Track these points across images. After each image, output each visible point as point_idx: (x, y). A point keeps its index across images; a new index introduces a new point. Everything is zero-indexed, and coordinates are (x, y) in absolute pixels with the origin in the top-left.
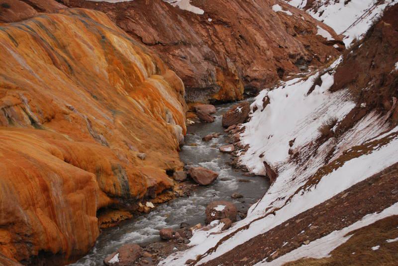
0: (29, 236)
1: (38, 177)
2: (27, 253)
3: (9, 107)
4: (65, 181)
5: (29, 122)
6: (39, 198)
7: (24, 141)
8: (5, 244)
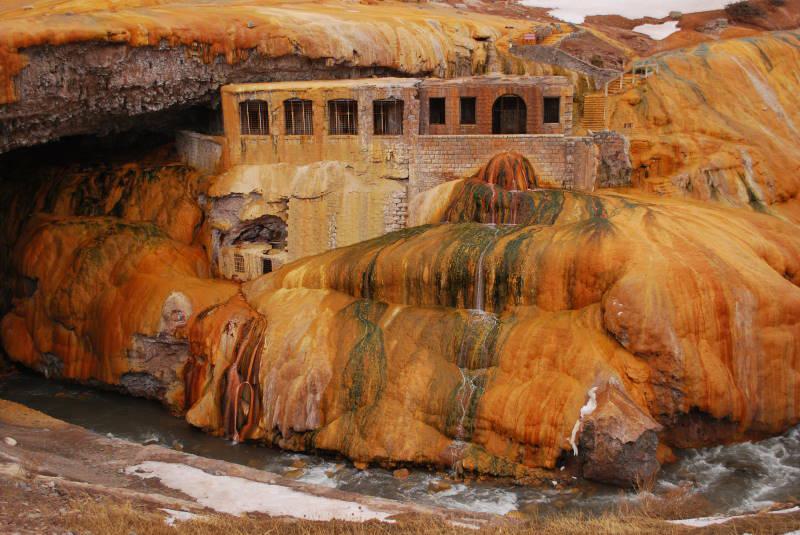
0: (677, 380)
1: (716, 288)
2: (671, 405)
3: (717, 170)
4: (762, 305)
5: (745, 198)
6: (708, 324)
7: (719, 228)
8: (638, 383)
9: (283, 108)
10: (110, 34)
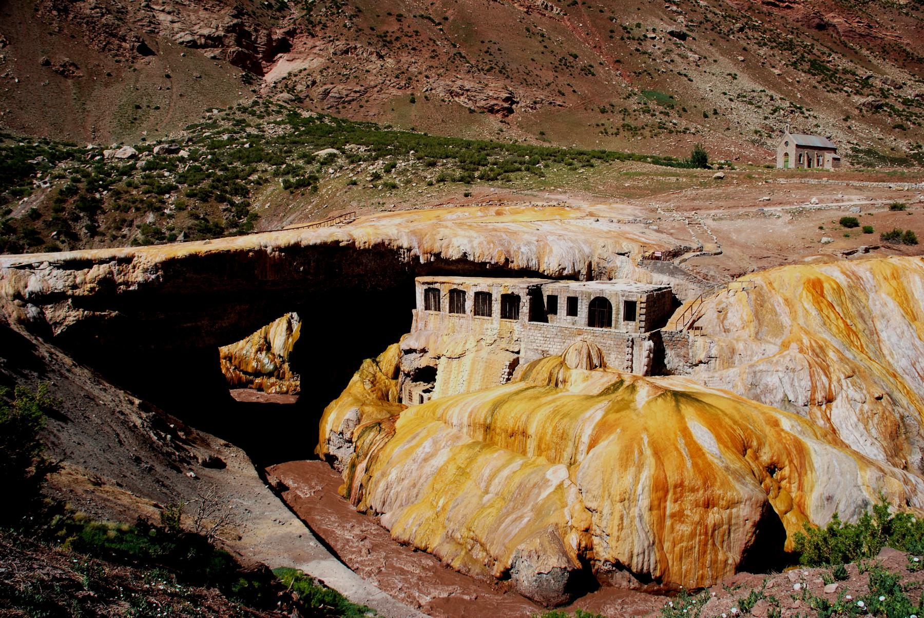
9: (448, 295)
10: (338, 242)
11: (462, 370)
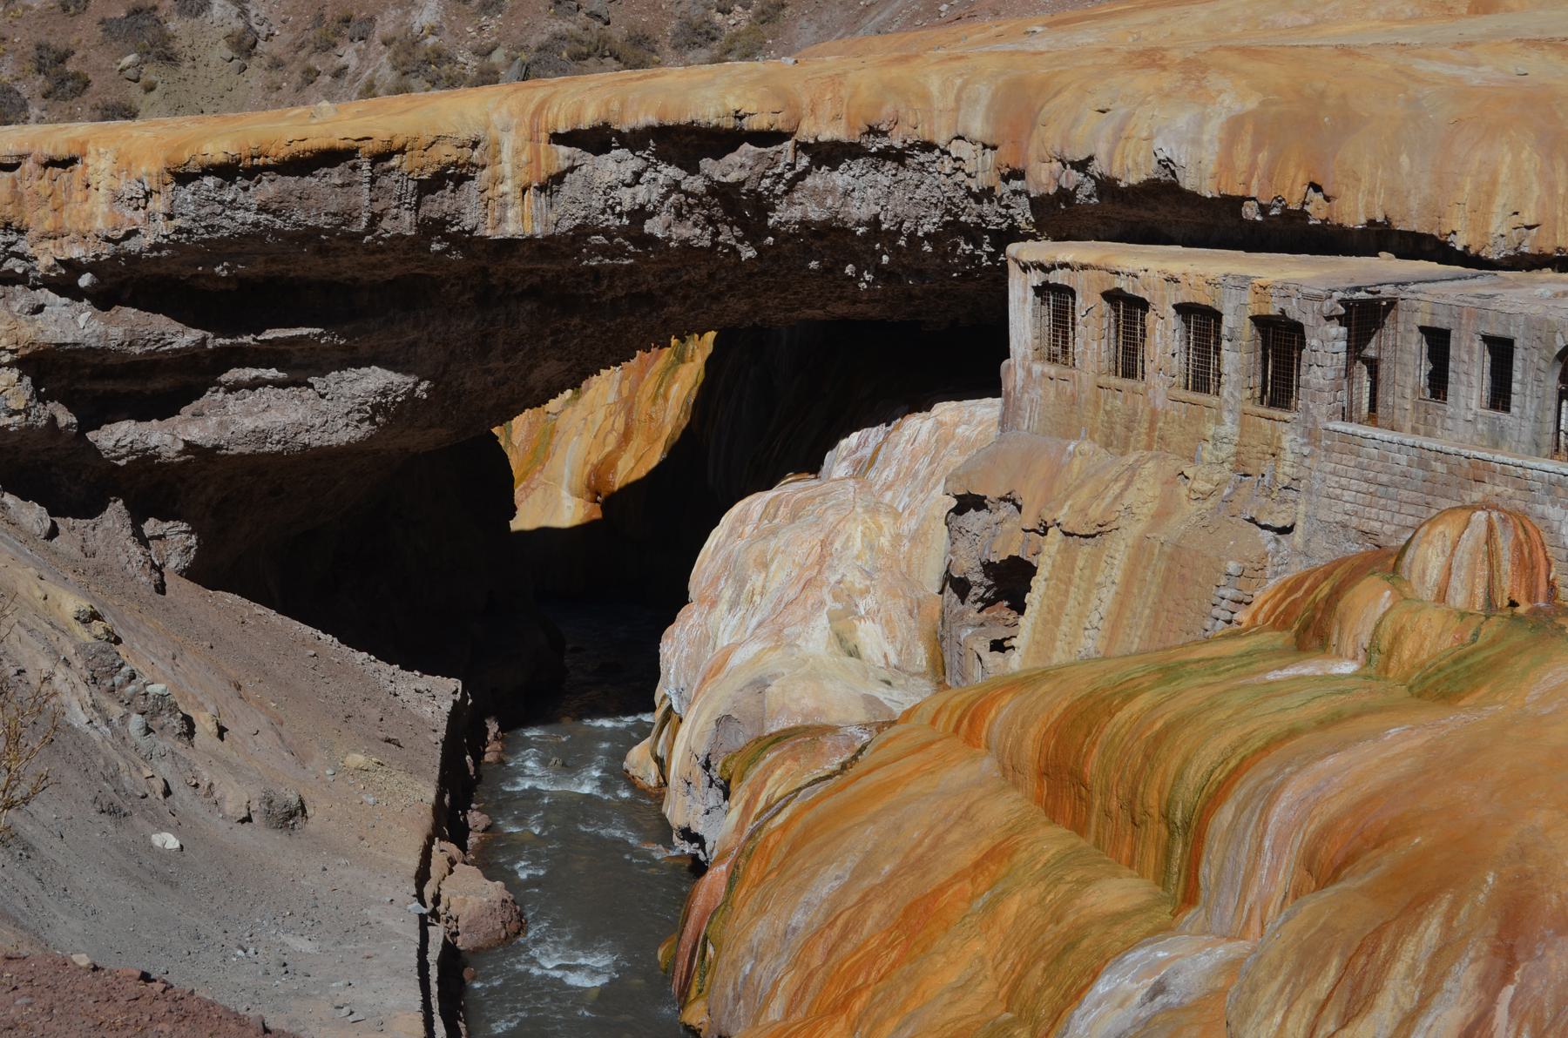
11: (1098, 580)
